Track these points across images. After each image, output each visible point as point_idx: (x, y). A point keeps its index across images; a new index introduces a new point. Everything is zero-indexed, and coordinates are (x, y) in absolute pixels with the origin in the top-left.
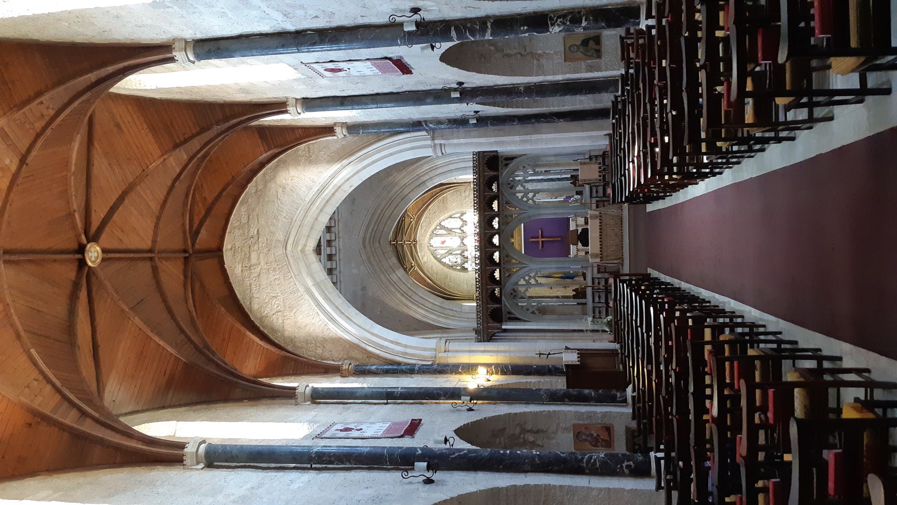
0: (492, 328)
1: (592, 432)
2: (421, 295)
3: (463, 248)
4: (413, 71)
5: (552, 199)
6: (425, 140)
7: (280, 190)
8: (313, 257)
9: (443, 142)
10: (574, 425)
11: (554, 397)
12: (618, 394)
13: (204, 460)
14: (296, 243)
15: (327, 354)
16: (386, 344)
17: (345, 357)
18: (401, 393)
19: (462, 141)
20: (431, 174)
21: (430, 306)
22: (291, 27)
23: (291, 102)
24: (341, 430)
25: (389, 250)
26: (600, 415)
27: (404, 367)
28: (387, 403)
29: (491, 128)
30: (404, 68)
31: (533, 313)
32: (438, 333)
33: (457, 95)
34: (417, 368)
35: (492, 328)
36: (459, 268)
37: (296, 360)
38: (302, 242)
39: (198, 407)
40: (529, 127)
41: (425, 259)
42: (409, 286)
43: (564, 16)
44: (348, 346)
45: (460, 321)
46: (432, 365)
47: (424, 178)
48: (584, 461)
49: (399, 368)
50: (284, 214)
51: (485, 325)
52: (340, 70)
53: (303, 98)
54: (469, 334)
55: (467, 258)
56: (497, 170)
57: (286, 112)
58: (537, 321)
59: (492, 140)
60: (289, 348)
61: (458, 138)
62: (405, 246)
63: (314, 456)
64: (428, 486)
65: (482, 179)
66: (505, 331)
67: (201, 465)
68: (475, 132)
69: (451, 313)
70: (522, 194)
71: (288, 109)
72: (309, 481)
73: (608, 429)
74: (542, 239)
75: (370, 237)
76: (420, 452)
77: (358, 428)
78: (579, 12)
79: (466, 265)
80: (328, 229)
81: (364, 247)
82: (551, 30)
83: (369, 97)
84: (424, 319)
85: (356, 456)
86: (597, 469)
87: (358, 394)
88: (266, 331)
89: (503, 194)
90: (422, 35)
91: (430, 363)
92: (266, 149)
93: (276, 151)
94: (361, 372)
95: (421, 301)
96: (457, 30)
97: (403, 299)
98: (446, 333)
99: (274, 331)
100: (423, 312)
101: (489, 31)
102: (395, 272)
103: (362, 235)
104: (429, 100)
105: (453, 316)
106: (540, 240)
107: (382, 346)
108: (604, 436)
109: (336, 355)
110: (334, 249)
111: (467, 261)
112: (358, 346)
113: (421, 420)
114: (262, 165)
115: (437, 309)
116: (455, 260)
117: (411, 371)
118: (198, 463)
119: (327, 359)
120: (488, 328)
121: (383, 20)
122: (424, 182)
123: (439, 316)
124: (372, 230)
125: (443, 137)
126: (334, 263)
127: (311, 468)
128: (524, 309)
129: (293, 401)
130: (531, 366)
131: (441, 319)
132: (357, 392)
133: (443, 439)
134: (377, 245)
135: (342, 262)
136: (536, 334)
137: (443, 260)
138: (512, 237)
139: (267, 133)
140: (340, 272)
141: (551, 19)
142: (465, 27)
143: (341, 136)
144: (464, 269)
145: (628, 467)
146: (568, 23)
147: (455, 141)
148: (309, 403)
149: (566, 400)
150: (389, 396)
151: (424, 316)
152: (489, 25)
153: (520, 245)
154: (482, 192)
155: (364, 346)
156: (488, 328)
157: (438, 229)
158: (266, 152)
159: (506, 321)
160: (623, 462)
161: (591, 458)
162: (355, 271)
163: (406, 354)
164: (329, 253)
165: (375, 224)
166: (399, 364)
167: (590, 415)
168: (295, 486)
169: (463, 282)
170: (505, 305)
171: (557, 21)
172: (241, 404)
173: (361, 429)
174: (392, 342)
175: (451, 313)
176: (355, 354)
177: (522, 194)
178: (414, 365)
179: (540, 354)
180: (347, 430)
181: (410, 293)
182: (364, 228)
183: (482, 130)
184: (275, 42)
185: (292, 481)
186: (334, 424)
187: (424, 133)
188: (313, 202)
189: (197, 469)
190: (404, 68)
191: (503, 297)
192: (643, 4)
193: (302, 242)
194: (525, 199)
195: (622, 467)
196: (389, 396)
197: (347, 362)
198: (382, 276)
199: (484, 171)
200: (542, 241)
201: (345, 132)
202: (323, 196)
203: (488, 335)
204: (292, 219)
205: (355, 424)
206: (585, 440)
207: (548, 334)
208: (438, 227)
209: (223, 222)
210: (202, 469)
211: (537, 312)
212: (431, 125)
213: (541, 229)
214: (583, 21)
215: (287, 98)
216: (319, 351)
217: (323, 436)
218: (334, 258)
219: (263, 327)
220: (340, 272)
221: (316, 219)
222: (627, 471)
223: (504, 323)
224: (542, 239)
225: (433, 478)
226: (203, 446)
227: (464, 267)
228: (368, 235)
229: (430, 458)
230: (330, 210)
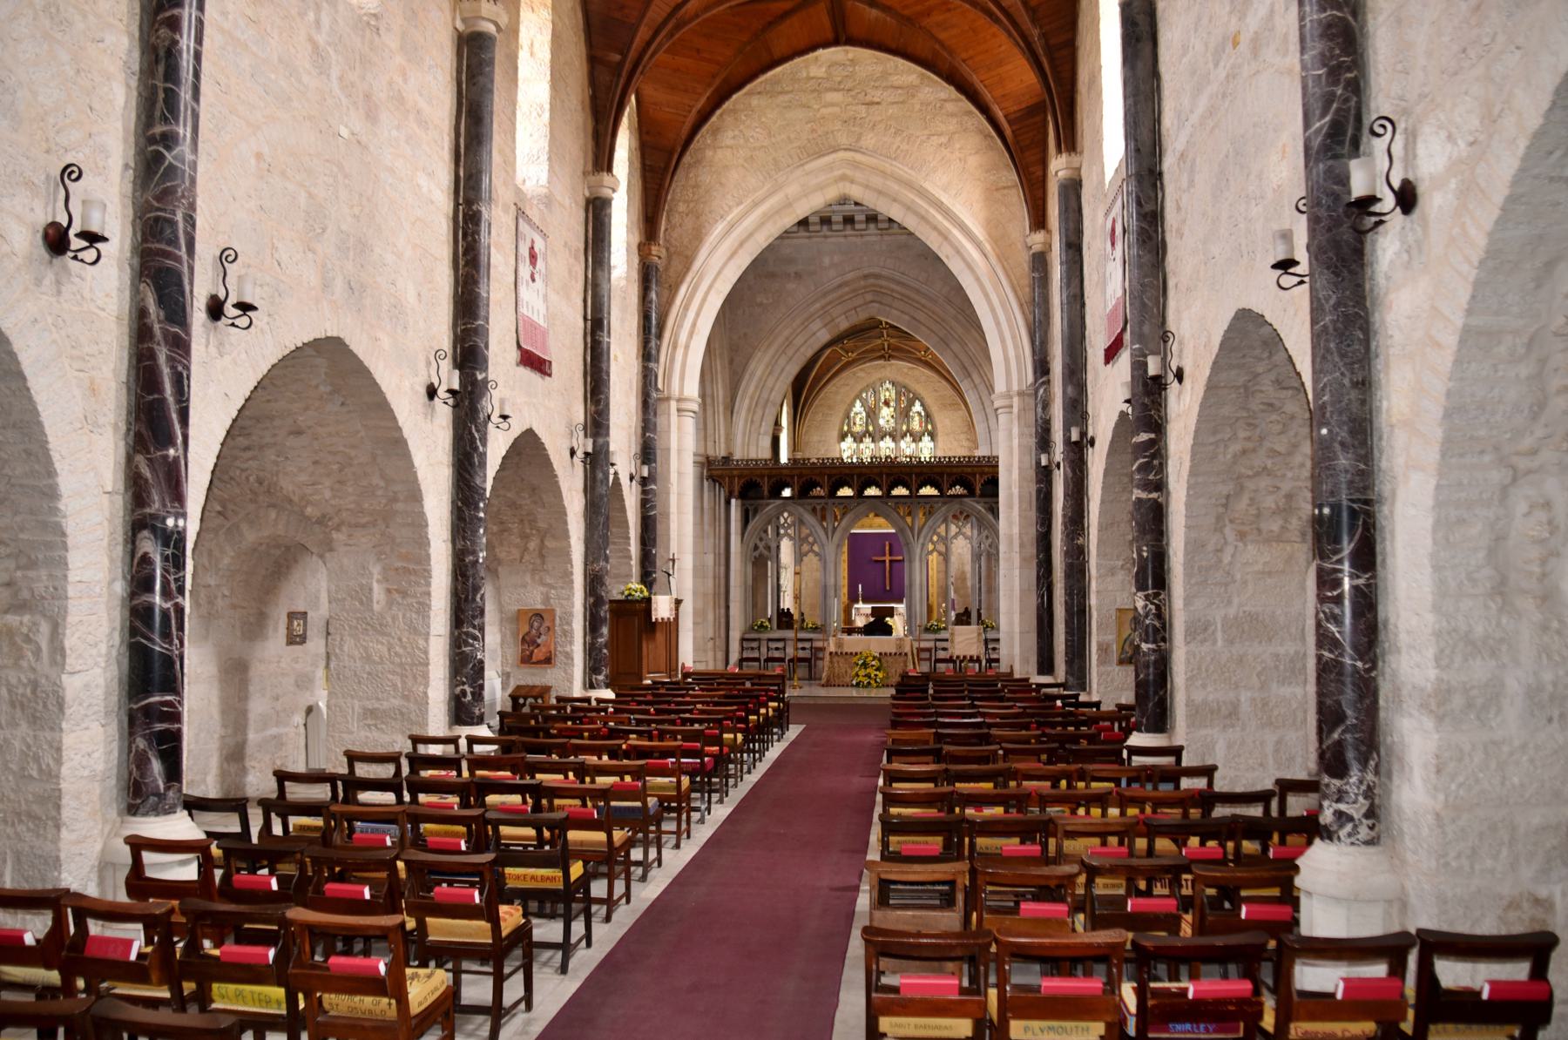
0: (731, 483)
1: (543, 637)
2: (788, 368)
3: (877, 437)
4: (1109, 366)
6: (1020, 380)
7: (944, 139)
8: (832, 193)
9: (1015, 410)
10: (552, 612)
11: (594, 582)
12: (601, 677)
13: (469, 30)
14: (856, 165)
15: (676, 219)
16: (691, 314)
17: (672, 250)
18: (600, 343)
19: (1016, 442)
20: (982, 387)
21: (770, 383)
22: (1169, 163)
23: (1075, 159)
24: (532, 248)
25: (861, 316)
26: (568, 649)
27: (653, 344)
28: (585, 319)
29: (1033, 488)
30: (1111, 354)
31: (756, 548)
32: (725, 397)
33: (1075, 436)
34: (652, 365)
35: (731, 483)
36: (846, 428)
37: (666, 168)
38: (858, 175)
39: (580, 15)
40: (1032, 550)
41: (861, 374)
42: (802, 350)
43: (1159, 615)
44: (689, 253)
45: (744, 434)
46: (657, 390)
47: (975, 376)
48: (471, 630)
49: (653, 338)
50: (904, 147)
51: (735, 472)
52: (1113, 244)
53: (1081, 181)
54: (723, 446)
56: (982, 496)
57: (1059, 151)
58: (744, 555)
59: (1016, 491)
60: (687, 159)
61: (1021, 435)
62: (879, 341)
63: (474, 208)
64: (423, 391)
65: (969, 470)
66: (728, 503)
67: (460, 26)
68: (1030, 462)
69: (757, 417)
70: (944, 534)
71: (1064, 155)
72: (432, 202)
73: (548, 661)
75: (881, 287)
76: (480, 377)
77: (537, 276)
78: (1164, 640)
79: (849, 439)
80: (872, 218)
81: (866, 277)
82: (1139, 594)
83: (1078, 291)
84: (747, 376)
85: (473, 276)
86: (460, 647)
87: (599, 273)
88: (714, 119)
89: (945, 503)
90: (1145, 384)
91: (660, 386)
92: (1013, 116)
93: (1008, 131)
94: (647, 275)
95: (778, 370)
96: (1152, 442)
97: (781, 339)
98: (725, 408)
99: (716, 131)
100: (759, 373)
101: (1144, 495)
102: (825, 326)
103: (885, 272)
104: (1070, 389)
105: (752, 421)
106: (887, 558)
107: (686, 309)
108: (539, 654)
109: (675, 235)
110: (863, 226)
112: (688, 269)
113: (550, 375)
114: (984, 109)
115: (765, 395)
117: (648, 355)
118: (464, 20)
119: (668, 220)
120: (731, 478)
121: (1172, 324)
122: (970, 376)
123: (752, 398)
124: (893, 290)
125: (1022, 410)
126: (840, 227)
127: (457, 205)
128: (763, 535)
129: (590, 167)
130: (654, 546)
131: (747, 401)
132: (603, 270)
133: (506, 413)
134: (869, 297)
135: (842, 240)
136: (722, 551)
137: (858, 404)
138: (876, 515)
139: (1037, 119)
140: (826, 237)
141: (1156, 595)
142: (1153, 456)
143: (1029, 241)
144: (843, 437)
145: (464, 693)
146: (1147, 622)
147: (1016, 431)
148: (587, 194)
149: (592, 600)
150: (596, 324)
151: (753, 374)
152: (1154, 495)
154: (948, 470)
155: (688, 279)
156: (731, 478)
158: (1005, 116)
159: (743, 505)
160: (471, 686)
161: (475, 638)
162: (826, 261)
163: (675, 347)
164: (857, 218)
165: (903, 295)
166: (660, 336)
167: (568, 634)
168: (422, 180)
170: (768, 505)
171: (1152, 603)
172: (586, 83)
173: (533, 280)
174: (694, 325)
175: (757, 417)
176: (676, 264)
177: (944, 534)
178: (657, 361)
179: (673, 560)
180: (533, 257)
181: (790, 352)
182: (897, 276)
183: (1032, 473)
184: (1145, 134)
185: (431, 175)
186: (545, 236)
187: (1030, 378)
188: (923, 193)
189: (454, 19)
190: (1111, 354)
191: (778, 502)
192: (1170, 738)
193: (858, 175)
194: (935, 538)
195: (464, 684)
196: (596, 324)
197: (663, 253)
198: (818, 305)
199: (982, 474)
201: (1037, 248)
202: (932, 211)
203: (721, 476)
204: (895, 159)
205: (543, 271)
206: (532, 627)
207: (723, 569)
209: (894, 46)
210: (456, 29)
211: (757, 554)
212: (1041, 391)
214: (1150, 646)
215: (1081, 153)
216: (682, 207)
217: (521, 220)
218: (849, 227)
219: (721, 115)
220: (826, 237)
221: (895, 200)
222: (458, 690)
223: (739, 502)
225: (436, 399)
226: (491, 28)
228: (883, 283)
229: (471, 393)
230: (910, 223)
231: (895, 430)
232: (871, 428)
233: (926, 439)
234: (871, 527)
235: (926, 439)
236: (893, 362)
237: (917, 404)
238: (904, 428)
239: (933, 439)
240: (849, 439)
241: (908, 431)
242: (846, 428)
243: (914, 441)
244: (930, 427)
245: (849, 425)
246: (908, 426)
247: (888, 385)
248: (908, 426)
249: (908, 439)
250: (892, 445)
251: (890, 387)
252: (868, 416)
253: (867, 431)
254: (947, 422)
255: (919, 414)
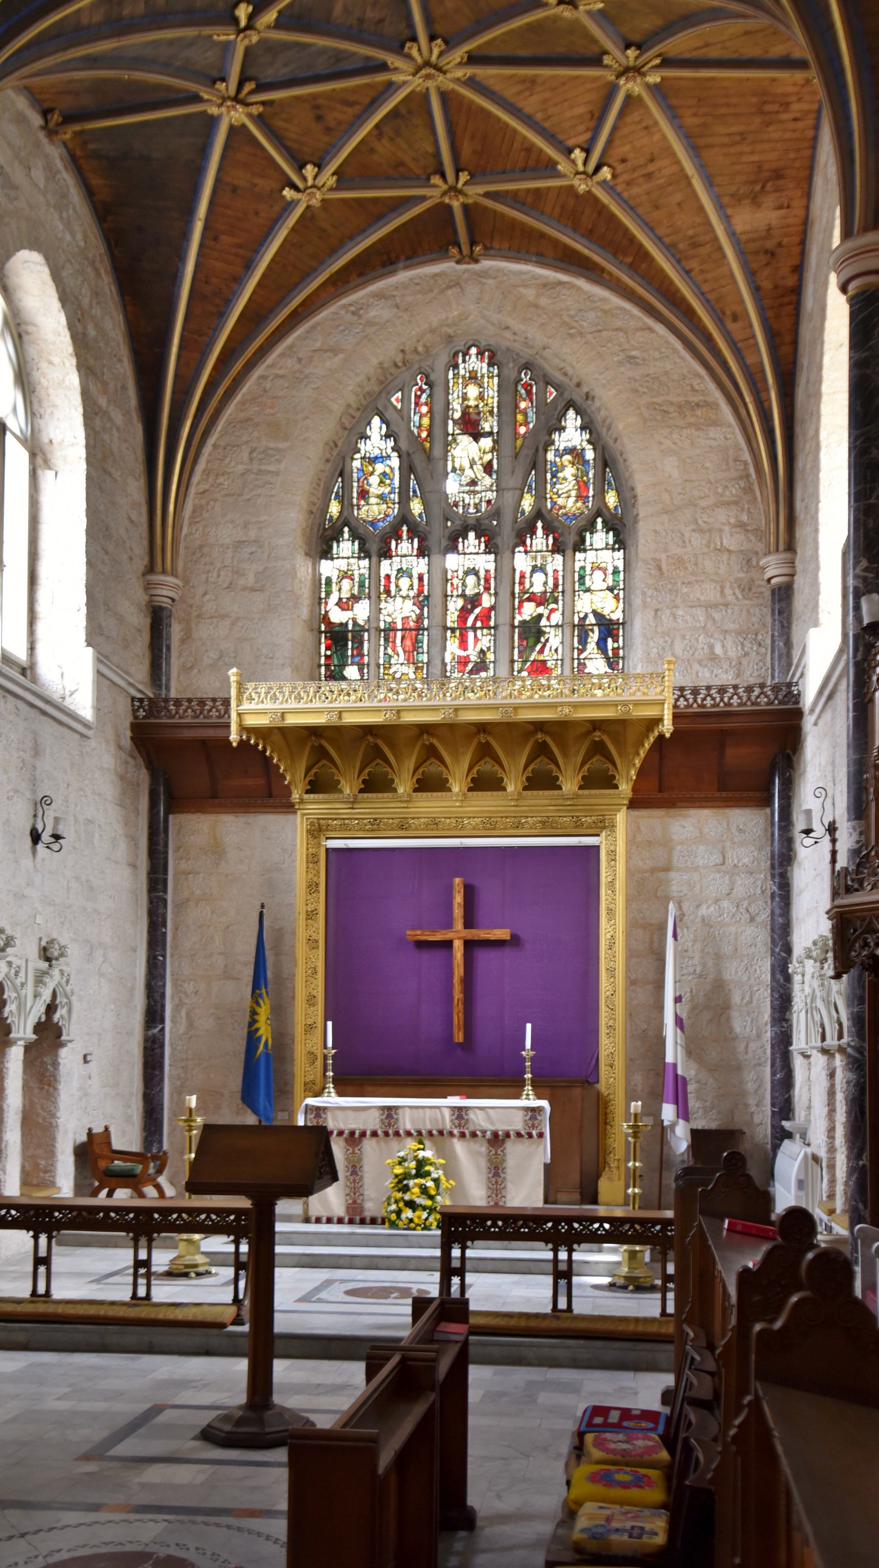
3: (437, 535)
5: (678, 1000)
36: (334, 508)
55: (386, 554)
74: (458, 945)
79: (346, 547)
106: (458, 934)
111: (368, 556)
116: (374, 485)
153: (434, 827)
157: (543, 394)
169: (246, 526)
200: (447, 945)
208: (552, 394)
213: (515, 941)
224: (458, 945)
227: (337, 536)
231: (496, 513)
232: (416, 507)
233: (600, 538)
234: (403, 828)
235: (600, 538)
236: (487, 264)
237: (572, 420)
238: (527, 503)
239: (620, 543)
240: (346, 547)
241: (538, 514)
242: (334, 508)
243: (557, 548)
244: (611, 499)
245: (344, 499)
246: (540, 496)
247: (474, 363)
248: (540, 496)
249: (540, 541)
250: (486, 563)
251: (482, 367)
252: (408, 468)
253: (405, 517)
254: (671, 467)
255: (576, 454)
